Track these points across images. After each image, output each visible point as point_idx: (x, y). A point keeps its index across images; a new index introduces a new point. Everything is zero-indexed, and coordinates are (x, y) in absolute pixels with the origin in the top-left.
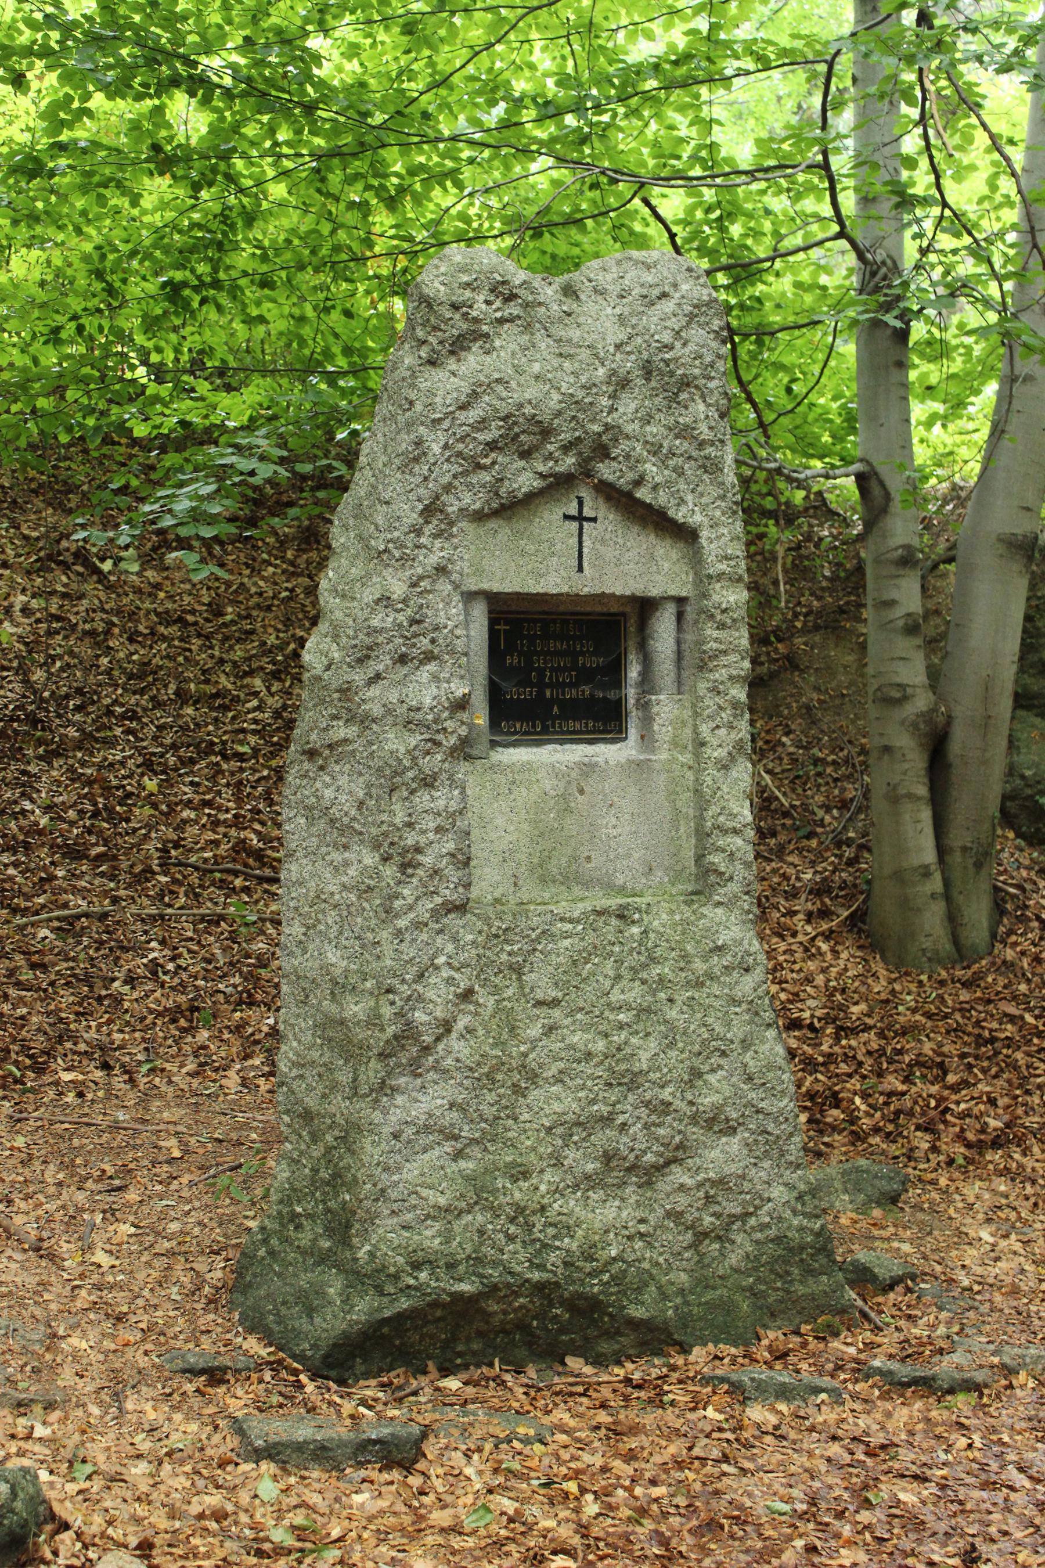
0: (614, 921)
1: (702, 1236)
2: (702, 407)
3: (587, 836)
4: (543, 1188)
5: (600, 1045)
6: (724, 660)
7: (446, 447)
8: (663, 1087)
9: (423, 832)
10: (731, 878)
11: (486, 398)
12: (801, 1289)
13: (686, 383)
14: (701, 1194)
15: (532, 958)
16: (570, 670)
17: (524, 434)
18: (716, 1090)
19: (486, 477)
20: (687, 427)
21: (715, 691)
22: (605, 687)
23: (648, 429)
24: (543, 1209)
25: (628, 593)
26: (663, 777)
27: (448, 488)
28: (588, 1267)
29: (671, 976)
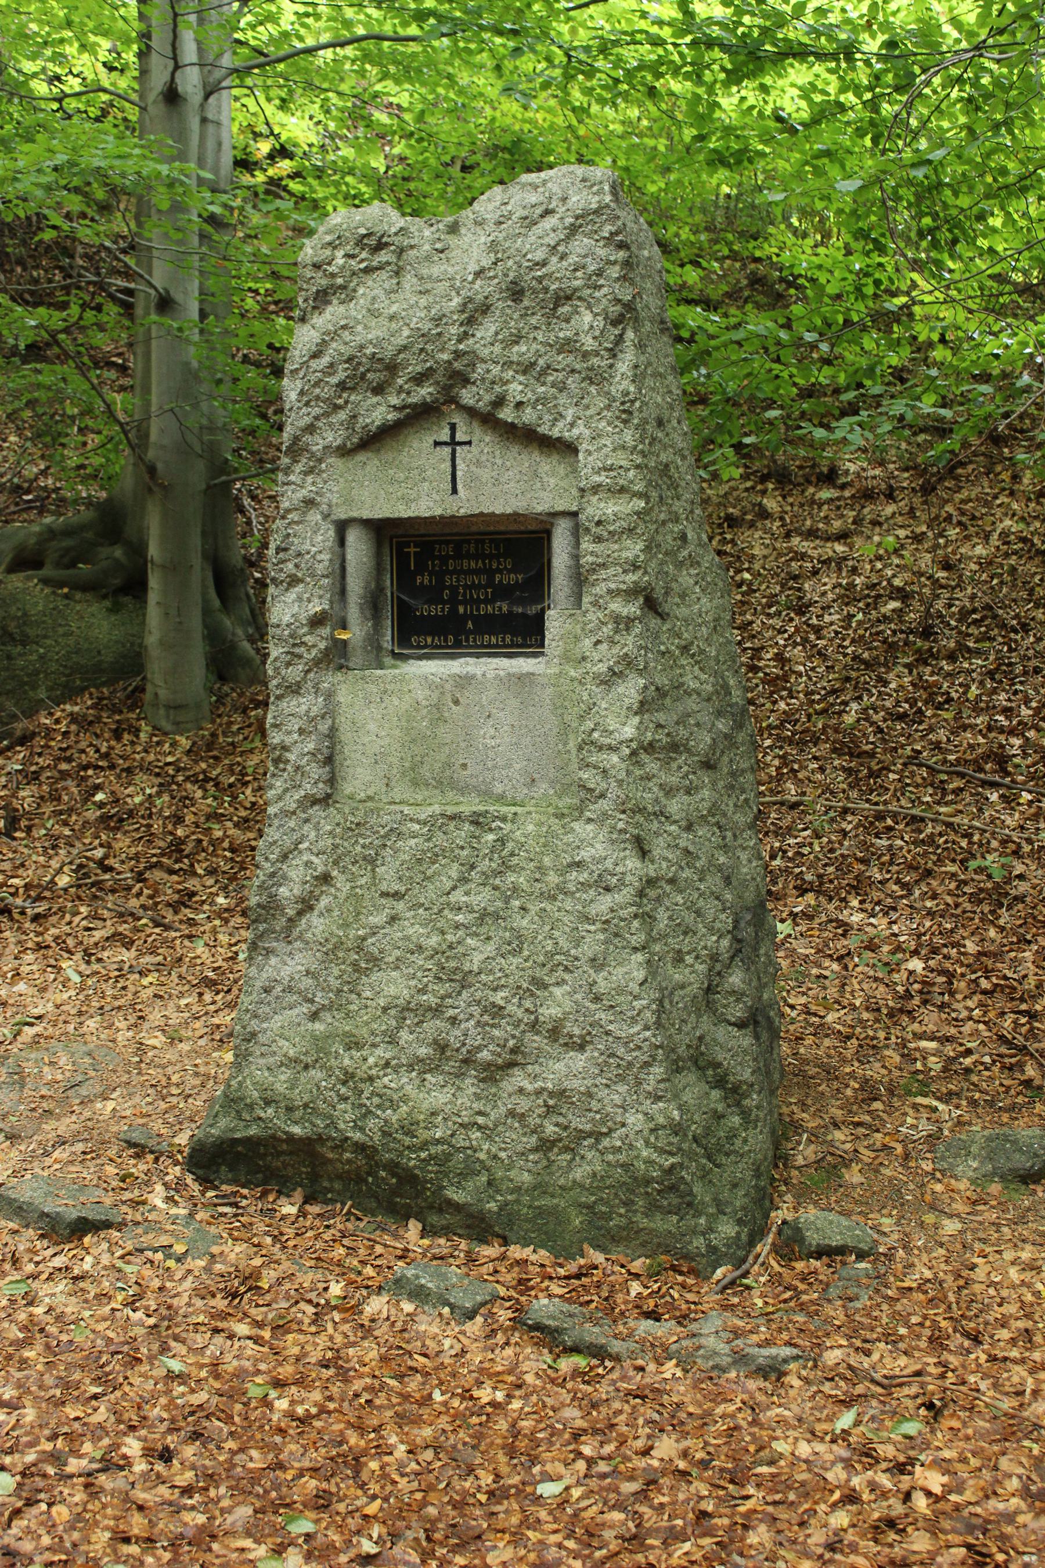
0: (467, 826)
1: (545, 1145)
2: (588, 318)
3: (463, 745)
4: (371, 1060)
5: (434, 941)
6: (603, 574)
7: (302, 393)
8: (495, 990)
9: (289, 733)
10: (602, 796)
11: (334, 345)
12: (644, 1223)
13: (563, 297)
14: (540, 1102)
15: (383, 853)
16: (485, 587)
17: (374, 373)
18: (557, 1003)
19: (342, 415)
20: (568, 341)
22: (522, 601)
23: (516, 349)
24: (371, 1079)
25: (509, 511)
26: (550, 690)
27: (310, 429)
28: (407, 1141)
29: (525, 886)
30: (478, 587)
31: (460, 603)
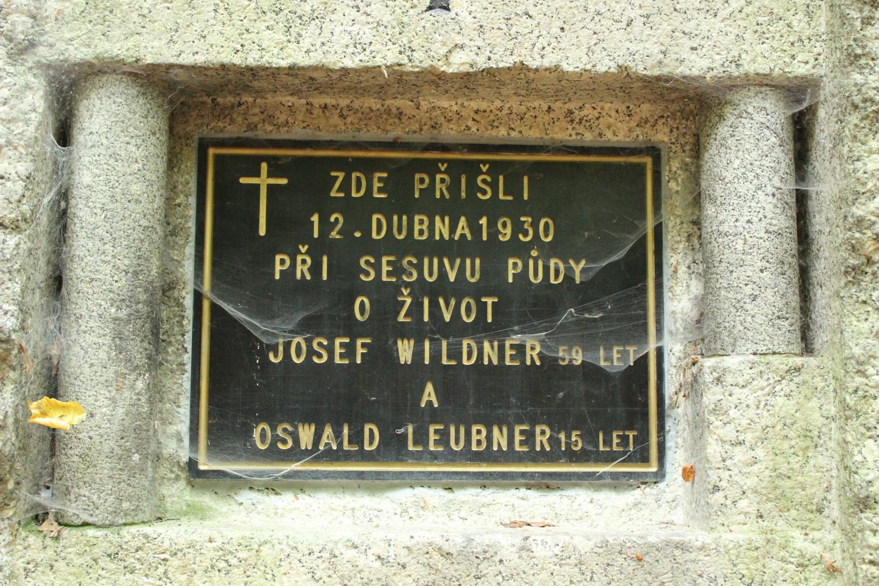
16: (478, 292)
22: (585, 333)
25: (605, 65)
30: (459, 289)
31: (403, 332)
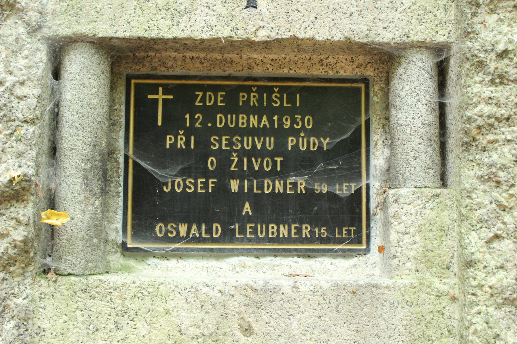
6: (506, 132)
16: (272, 155)
21: (492, 180)
22: (330, 177)
25: (338, 37)
26: (402, 312)
30: (263, 154)
31: (233, 176)
